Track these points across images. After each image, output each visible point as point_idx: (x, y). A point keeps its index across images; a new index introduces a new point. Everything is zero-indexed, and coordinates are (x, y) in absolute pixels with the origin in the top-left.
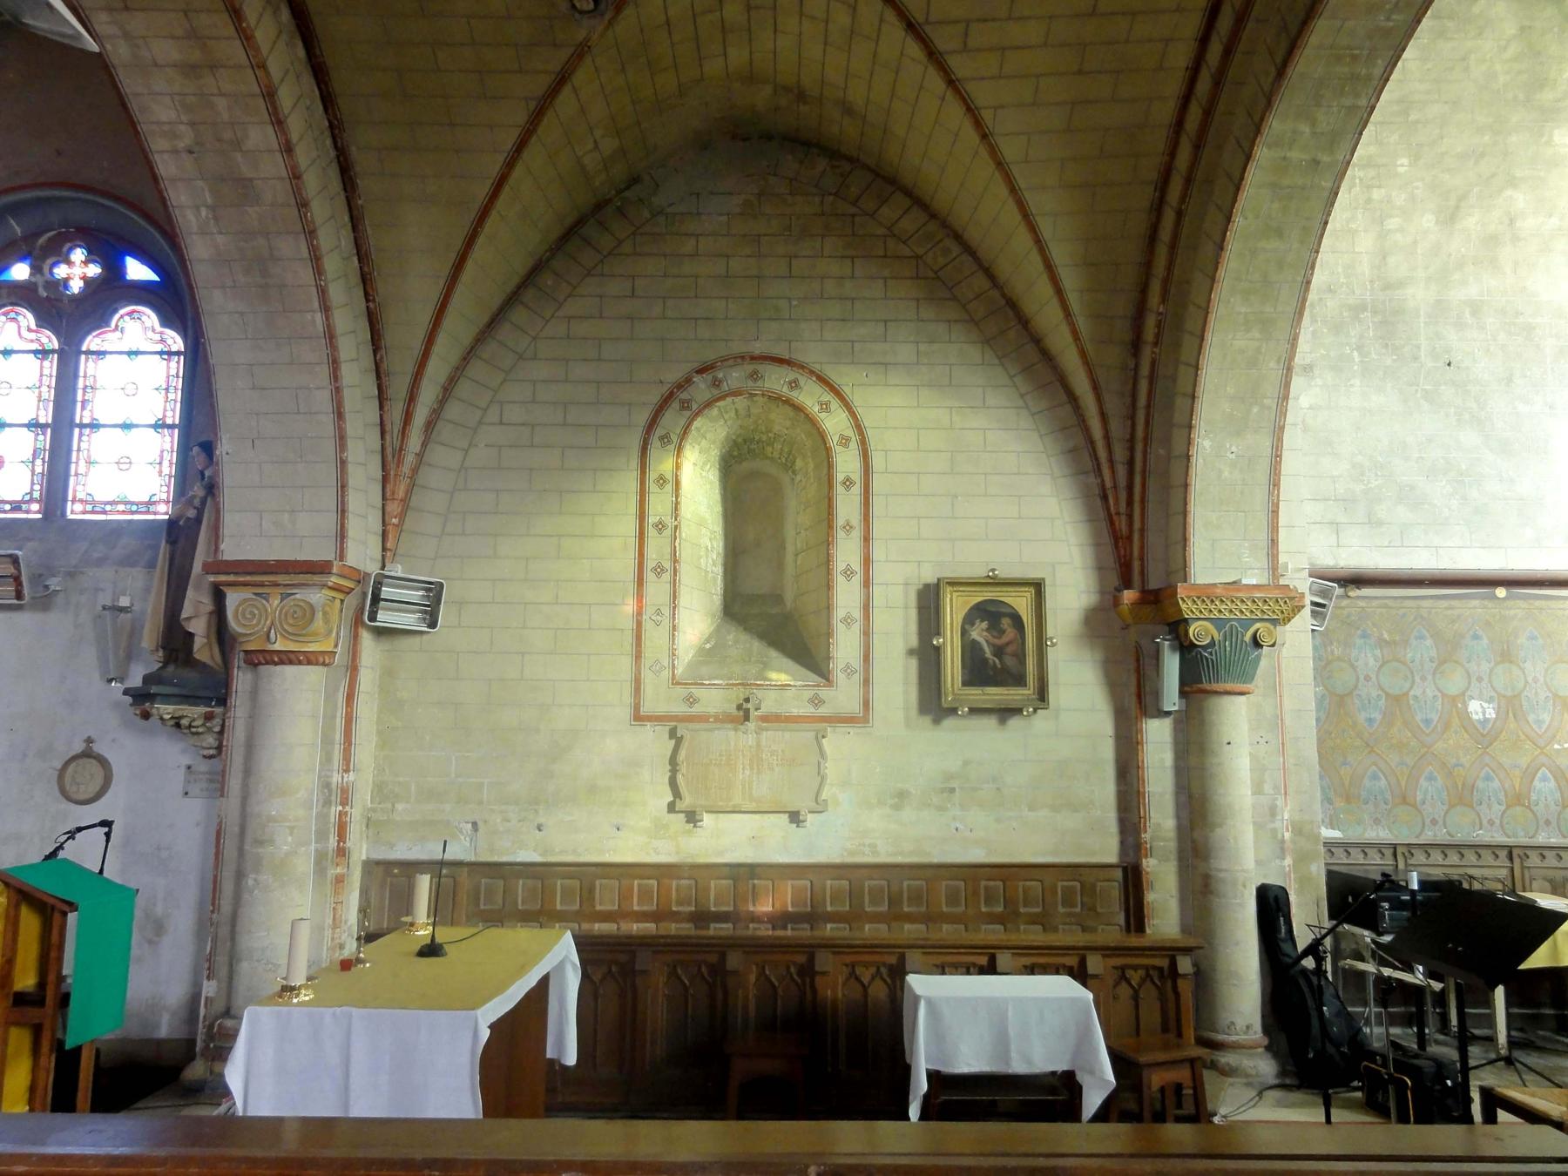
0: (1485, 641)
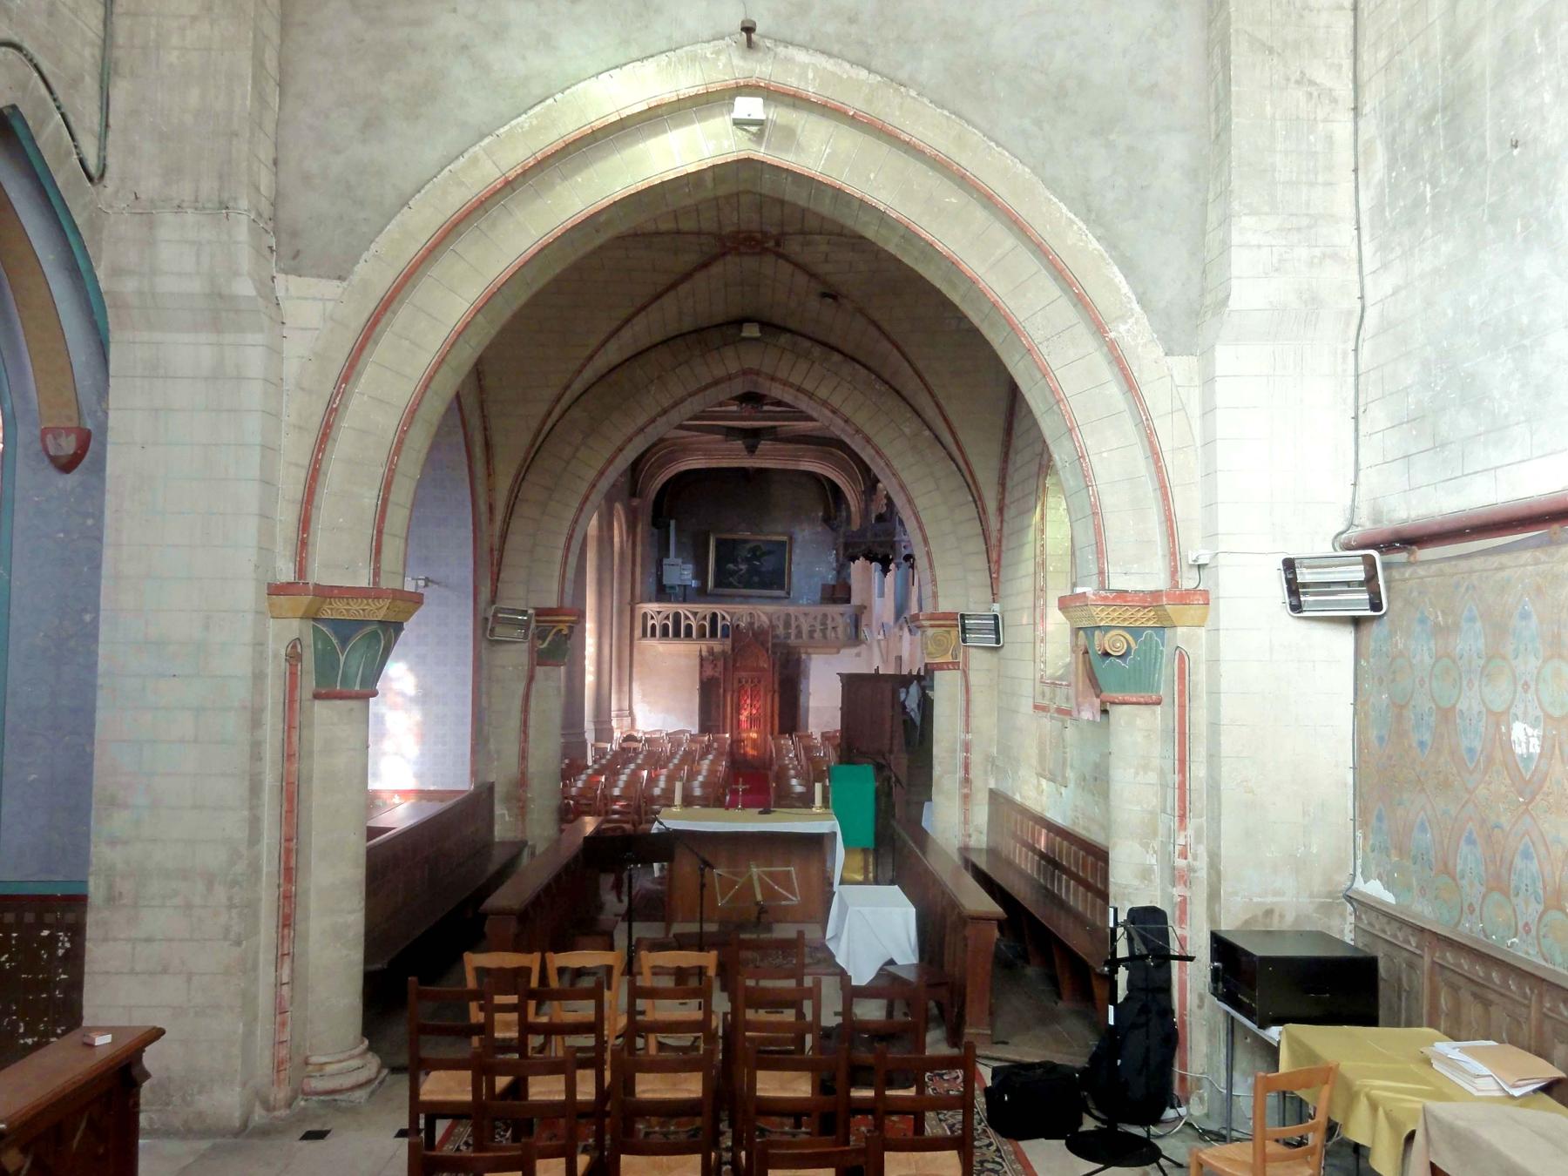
0: (1534, 619)
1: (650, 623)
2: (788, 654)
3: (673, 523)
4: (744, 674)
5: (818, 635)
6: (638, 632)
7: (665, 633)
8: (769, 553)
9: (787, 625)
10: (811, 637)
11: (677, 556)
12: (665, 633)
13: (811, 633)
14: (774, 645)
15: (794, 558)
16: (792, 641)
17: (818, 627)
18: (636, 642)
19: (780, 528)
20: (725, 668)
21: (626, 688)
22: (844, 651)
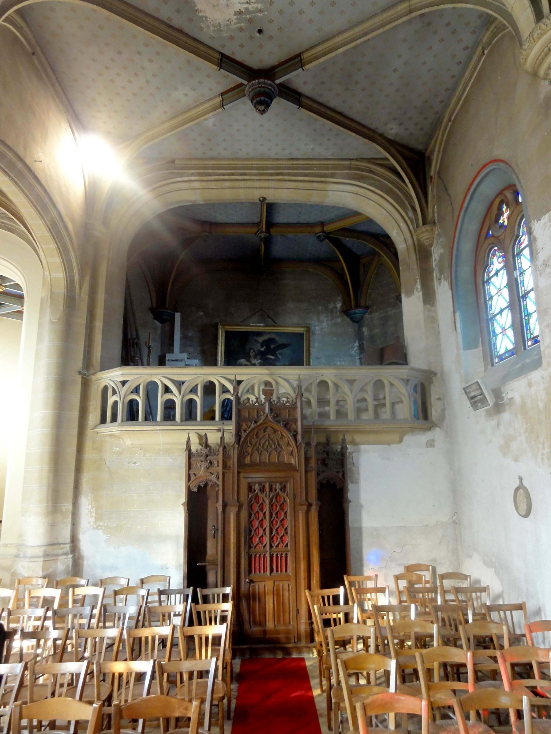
1: (111, 400)
2: (328, 443)
3: (178, 316)
4: (257, 477)
5: (368, 416)
6: (94, 416)
7: (132, 415)
8: (283, 346)
9: (323, 402)
10: (358, 417)
11: (182, 352)
12: (132, 415)
13: (359, 411)
14: (306, 431)
15: (313, 351)
16: (332, 422)
17: (371, 403)
18: (89, 432)
19: (295, 320)
20: (225, 466)
21: (68, 506)
22: (406, 438)
